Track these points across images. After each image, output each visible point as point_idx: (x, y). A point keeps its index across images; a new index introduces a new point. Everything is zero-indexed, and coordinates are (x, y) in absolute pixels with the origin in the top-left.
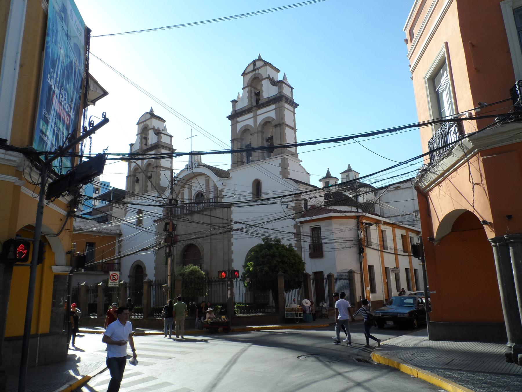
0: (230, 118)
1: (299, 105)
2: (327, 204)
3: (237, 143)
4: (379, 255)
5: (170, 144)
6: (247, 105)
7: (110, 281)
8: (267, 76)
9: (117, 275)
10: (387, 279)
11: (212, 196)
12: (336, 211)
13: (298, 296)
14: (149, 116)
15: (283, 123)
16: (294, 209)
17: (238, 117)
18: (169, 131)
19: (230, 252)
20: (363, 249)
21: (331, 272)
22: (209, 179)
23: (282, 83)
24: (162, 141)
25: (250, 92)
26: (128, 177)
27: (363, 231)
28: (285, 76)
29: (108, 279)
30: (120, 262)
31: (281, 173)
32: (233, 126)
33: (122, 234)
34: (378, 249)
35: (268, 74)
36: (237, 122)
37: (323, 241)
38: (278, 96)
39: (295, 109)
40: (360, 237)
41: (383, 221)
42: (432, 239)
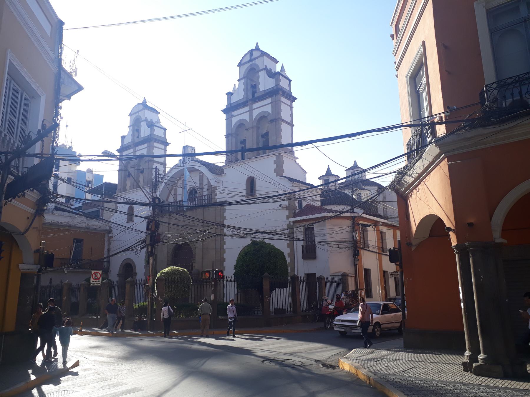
0: (224, 111)
1: (297, 99)
2: (323, 203)
3: (232, 139)
4: (377, 258)
5: (163, 137)
6: (242, 98)
7: (92, 280)
8: (264, 68)
9: (99, 273)
10: (385, 283)
11: (205, 193)
12: (331, 211)
13: (291, 298)
14: (141, 107)
15: (279, 118)
16: (288, 208)
17: (234, 111)
18: (164, 123)
19: (222, 251)
20: (358, 251)
21: (322, 274)
22: (203, 175)
23: (279, 75)
25: (246, 84)
26: (119, 171)
27: (358, 232)
28: (282, 67)
29: (90, 277)
30: (109, 260)
31: (275, 171)
32: (228, 120)
33: (111, 231)
34: (375, 251)
35: (265, 65)
36: (233, 116)
38: (274, 89)
39: (293, 103)
40: (355, 239)
41: (382, 222)
42: (409, 244)
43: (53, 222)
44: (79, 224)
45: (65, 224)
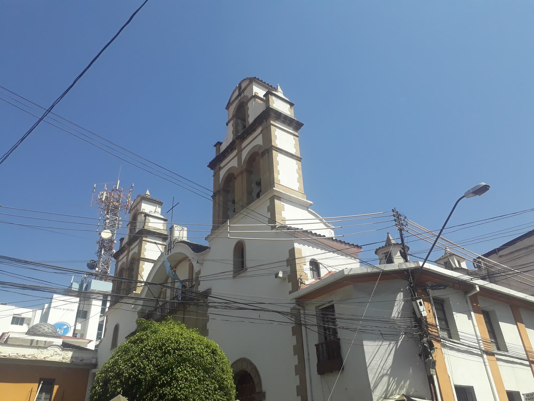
14: (139, 198)
15: (272, 146)
17: (221, 161)
20: (431, 346)
24: (149, 225)
25: (236, 126)
32: (216, 176)
36: (221, 168)
37: (341, 334)
43: (11, 355)
44: (51, 357)
45: (30, 357)
